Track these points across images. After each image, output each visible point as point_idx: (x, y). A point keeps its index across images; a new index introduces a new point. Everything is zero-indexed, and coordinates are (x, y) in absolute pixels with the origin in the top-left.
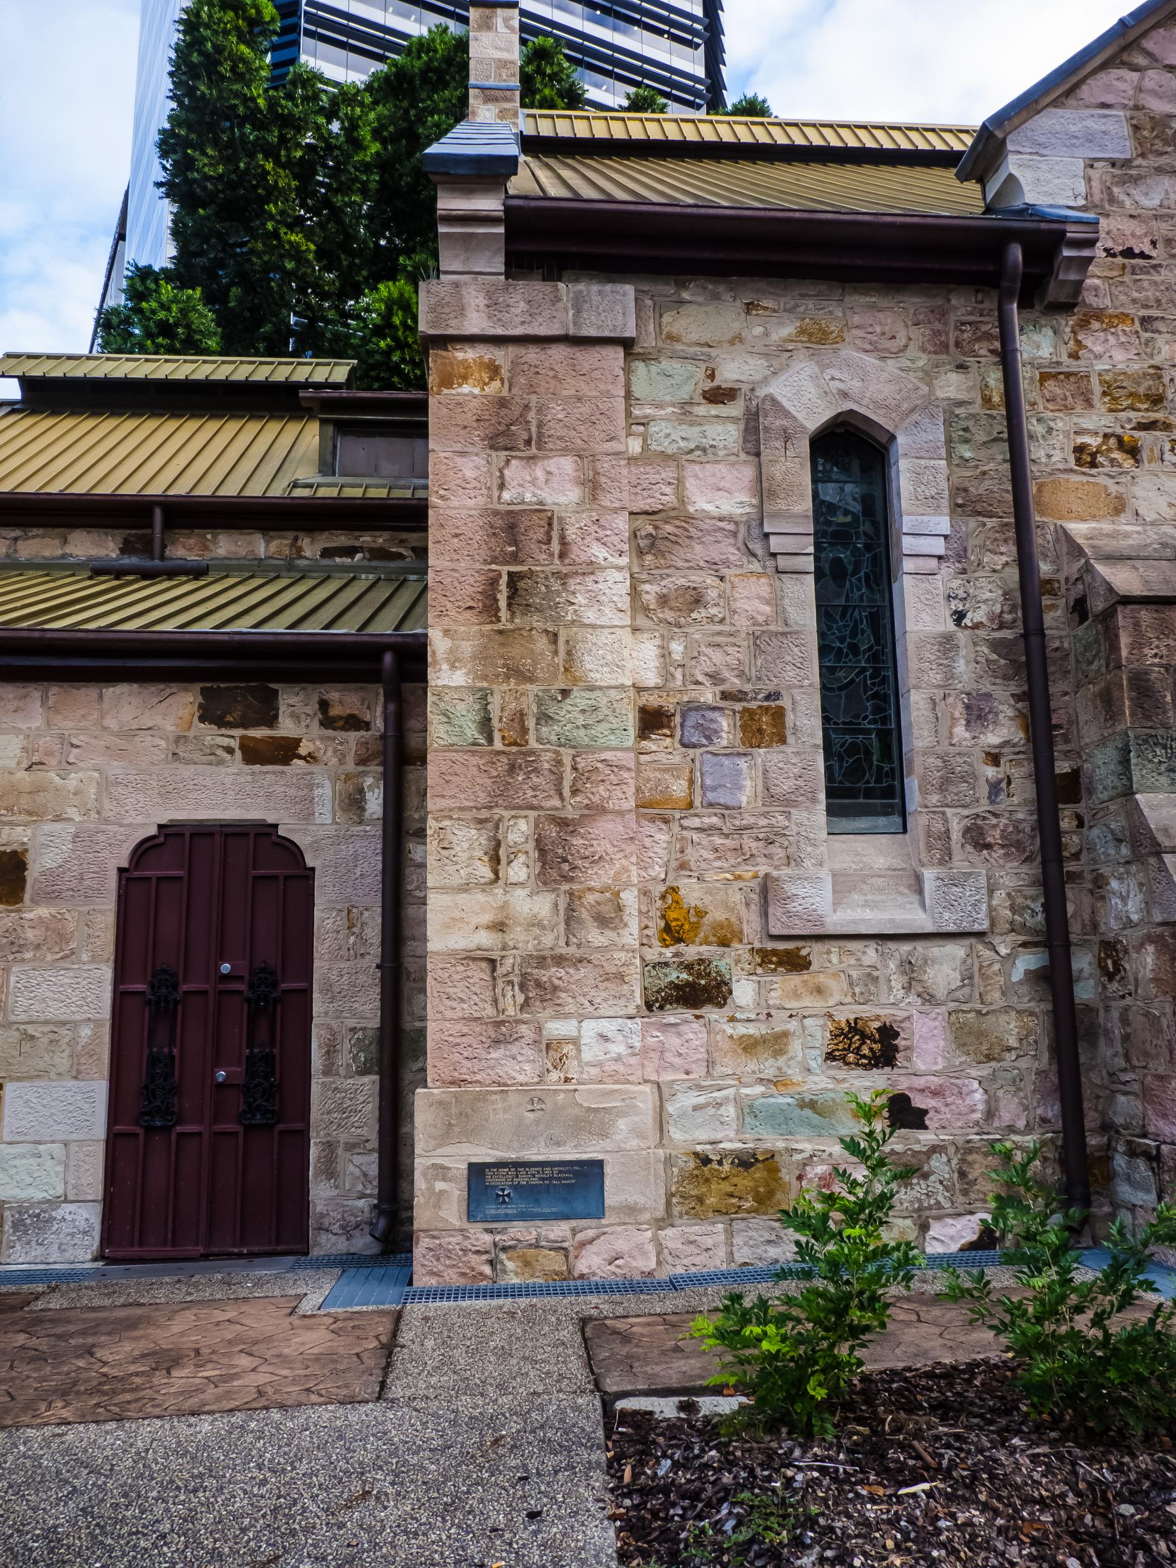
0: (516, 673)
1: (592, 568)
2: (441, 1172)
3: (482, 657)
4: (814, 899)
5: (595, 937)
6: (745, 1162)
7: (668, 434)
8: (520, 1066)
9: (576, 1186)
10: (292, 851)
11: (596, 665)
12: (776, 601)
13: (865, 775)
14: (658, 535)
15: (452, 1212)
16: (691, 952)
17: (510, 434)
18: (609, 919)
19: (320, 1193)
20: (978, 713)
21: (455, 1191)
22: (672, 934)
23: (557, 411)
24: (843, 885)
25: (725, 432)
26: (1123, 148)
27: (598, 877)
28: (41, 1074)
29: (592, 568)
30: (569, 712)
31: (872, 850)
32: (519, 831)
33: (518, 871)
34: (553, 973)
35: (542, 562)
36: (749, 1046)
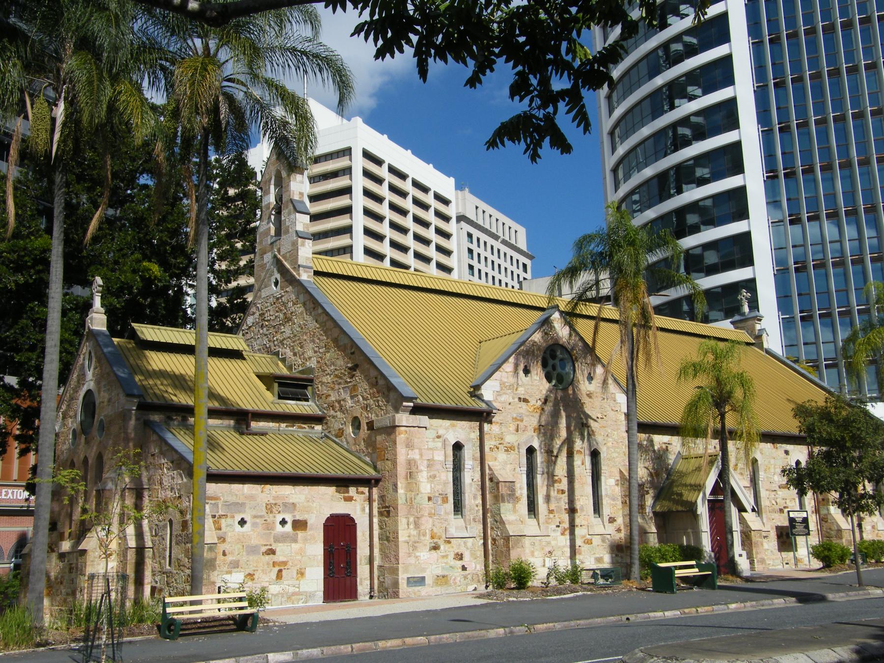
0: (411, 490)
1: (421, 471)
2: (403, 579)
3: (406, 487)
4: (453, 532)
5: (422, 538)
6: (443, 577)
7: (431, 445)
8: (412, 560)
9: (421, 581)
10: (352, 520)
11: (422, 490)
12: (447, 476)
13: (458, 507)
14: (431, 464)
15: (405, 585)
16: (435, 540)
17: (409, 445)
18: (424, 535)
19: (359, 588)
20: (475, 498)
21: (405, 582)
22: (432, 537)
23: (416, 440)
24: (457, 528)
25: (439, 444)
26: (498, 389)
27: (423, 527)
28: (312, 566)
29: (421, 471)
30: (418, 498)
31: (460, 521)
32: (411, 519)
33: (412, 526)
34: (417, 545)
35: (414, 469)
36: (443, 557)
